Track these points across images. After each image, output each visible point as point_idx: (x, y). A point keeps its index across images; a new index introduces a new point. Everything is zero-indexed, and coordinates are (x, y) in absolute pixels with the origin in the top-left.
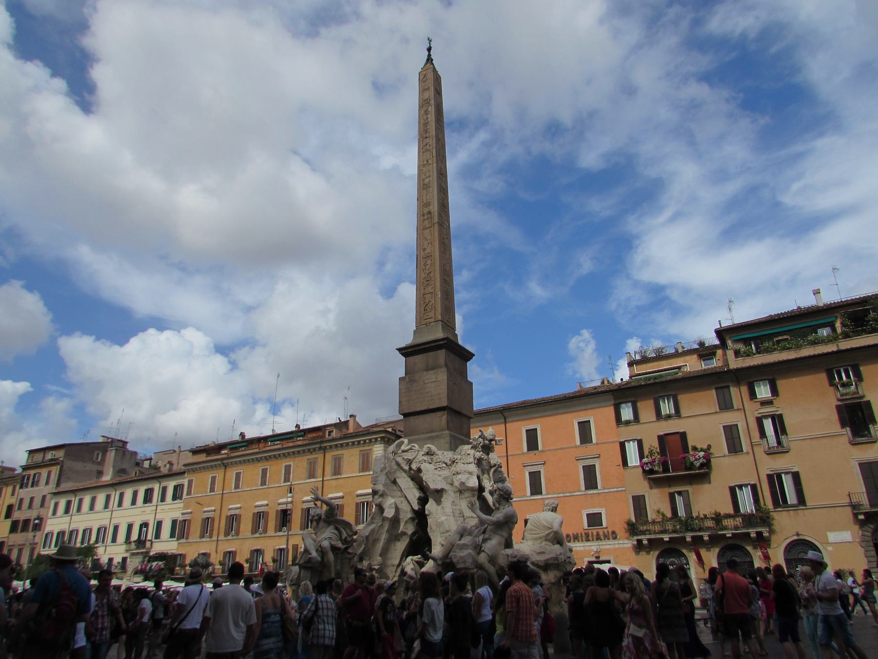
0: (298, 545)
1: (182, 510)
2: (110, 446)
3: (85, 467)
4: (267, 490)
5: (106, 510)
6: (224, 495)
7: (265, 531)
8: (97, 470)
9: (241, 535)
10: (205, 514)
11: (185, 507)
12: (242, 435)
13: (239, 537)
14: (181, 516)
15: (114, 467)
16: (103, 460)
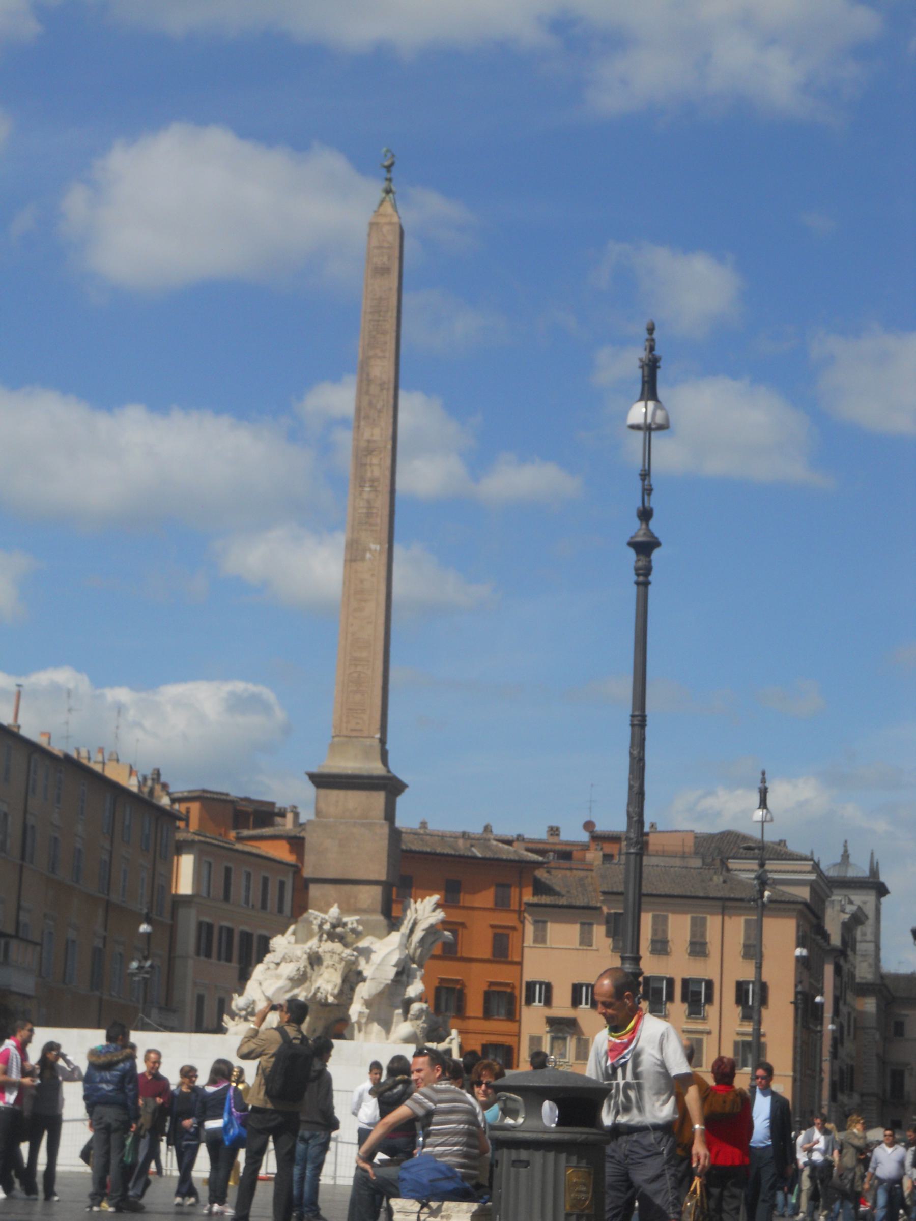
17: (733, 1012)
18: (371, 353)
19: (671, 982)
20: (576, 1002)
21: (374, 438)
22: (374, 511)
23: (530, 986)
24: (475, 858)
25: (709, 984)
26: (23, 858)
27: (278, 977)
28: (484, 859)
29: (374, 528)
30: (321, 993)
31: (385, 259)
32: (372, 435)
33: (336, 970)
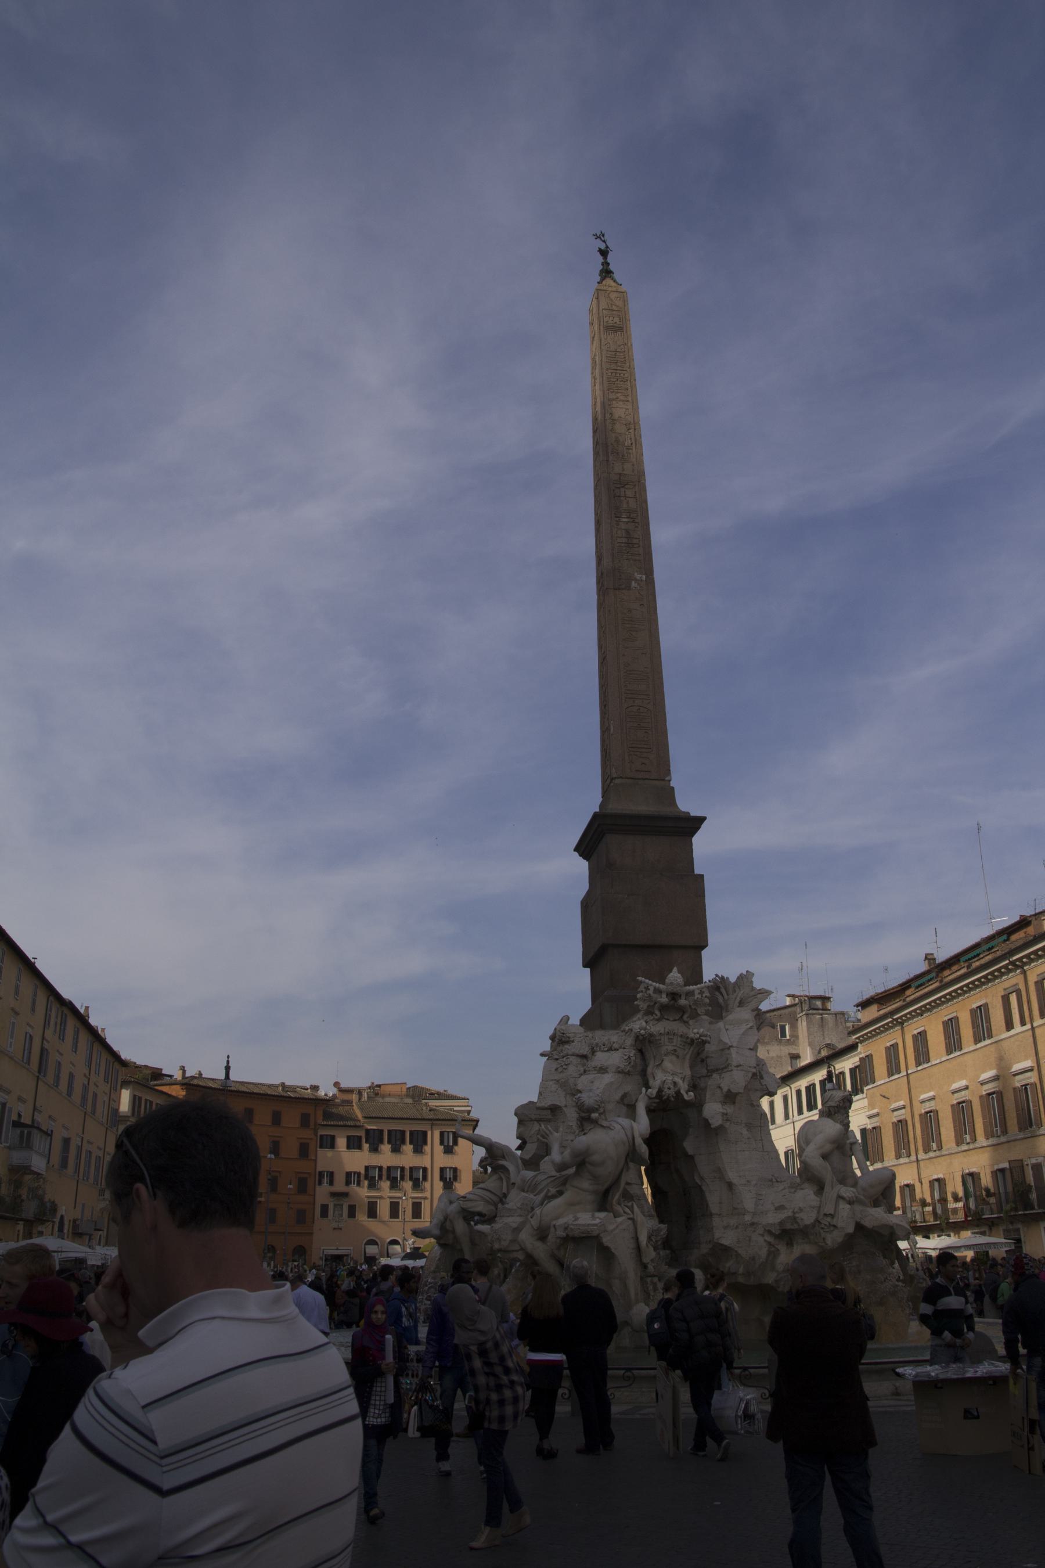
0: (1022, 1160)
1: (868, 1111)
2: (799, 1010)
3: (768, 1051)
4: (961, 1058)
5: (788, 1121)
6: (911, 1077)
7: (974, 1139)
8: (789, 1054)
9: (944, 1148)
10: (896, 1113)
11: (871, 1106)
12: (929, 958)
13: (944, 1152)
14: (868, 1121)
15: (811, 1044)
16: (795, 1036)
17: (439, 1185)
18: (612, 396)
19: (403, 1169)
20: (348, 1183)
21: (625, 472)
22: (635, 541)
23: (321, 1174)
24: (290, 1097)
25: (425, 1170)
26: (39, 1072)
27: (603, 1070)
28: (295, 1098)
29: (637, 558)
30: (669, 1088)
31: (616, 320)
32: (623, 470)
33: (678, 1057)
